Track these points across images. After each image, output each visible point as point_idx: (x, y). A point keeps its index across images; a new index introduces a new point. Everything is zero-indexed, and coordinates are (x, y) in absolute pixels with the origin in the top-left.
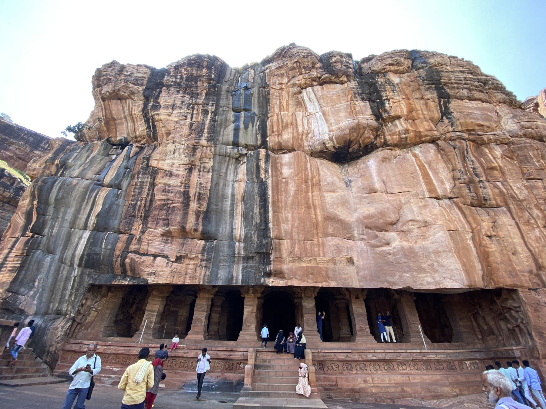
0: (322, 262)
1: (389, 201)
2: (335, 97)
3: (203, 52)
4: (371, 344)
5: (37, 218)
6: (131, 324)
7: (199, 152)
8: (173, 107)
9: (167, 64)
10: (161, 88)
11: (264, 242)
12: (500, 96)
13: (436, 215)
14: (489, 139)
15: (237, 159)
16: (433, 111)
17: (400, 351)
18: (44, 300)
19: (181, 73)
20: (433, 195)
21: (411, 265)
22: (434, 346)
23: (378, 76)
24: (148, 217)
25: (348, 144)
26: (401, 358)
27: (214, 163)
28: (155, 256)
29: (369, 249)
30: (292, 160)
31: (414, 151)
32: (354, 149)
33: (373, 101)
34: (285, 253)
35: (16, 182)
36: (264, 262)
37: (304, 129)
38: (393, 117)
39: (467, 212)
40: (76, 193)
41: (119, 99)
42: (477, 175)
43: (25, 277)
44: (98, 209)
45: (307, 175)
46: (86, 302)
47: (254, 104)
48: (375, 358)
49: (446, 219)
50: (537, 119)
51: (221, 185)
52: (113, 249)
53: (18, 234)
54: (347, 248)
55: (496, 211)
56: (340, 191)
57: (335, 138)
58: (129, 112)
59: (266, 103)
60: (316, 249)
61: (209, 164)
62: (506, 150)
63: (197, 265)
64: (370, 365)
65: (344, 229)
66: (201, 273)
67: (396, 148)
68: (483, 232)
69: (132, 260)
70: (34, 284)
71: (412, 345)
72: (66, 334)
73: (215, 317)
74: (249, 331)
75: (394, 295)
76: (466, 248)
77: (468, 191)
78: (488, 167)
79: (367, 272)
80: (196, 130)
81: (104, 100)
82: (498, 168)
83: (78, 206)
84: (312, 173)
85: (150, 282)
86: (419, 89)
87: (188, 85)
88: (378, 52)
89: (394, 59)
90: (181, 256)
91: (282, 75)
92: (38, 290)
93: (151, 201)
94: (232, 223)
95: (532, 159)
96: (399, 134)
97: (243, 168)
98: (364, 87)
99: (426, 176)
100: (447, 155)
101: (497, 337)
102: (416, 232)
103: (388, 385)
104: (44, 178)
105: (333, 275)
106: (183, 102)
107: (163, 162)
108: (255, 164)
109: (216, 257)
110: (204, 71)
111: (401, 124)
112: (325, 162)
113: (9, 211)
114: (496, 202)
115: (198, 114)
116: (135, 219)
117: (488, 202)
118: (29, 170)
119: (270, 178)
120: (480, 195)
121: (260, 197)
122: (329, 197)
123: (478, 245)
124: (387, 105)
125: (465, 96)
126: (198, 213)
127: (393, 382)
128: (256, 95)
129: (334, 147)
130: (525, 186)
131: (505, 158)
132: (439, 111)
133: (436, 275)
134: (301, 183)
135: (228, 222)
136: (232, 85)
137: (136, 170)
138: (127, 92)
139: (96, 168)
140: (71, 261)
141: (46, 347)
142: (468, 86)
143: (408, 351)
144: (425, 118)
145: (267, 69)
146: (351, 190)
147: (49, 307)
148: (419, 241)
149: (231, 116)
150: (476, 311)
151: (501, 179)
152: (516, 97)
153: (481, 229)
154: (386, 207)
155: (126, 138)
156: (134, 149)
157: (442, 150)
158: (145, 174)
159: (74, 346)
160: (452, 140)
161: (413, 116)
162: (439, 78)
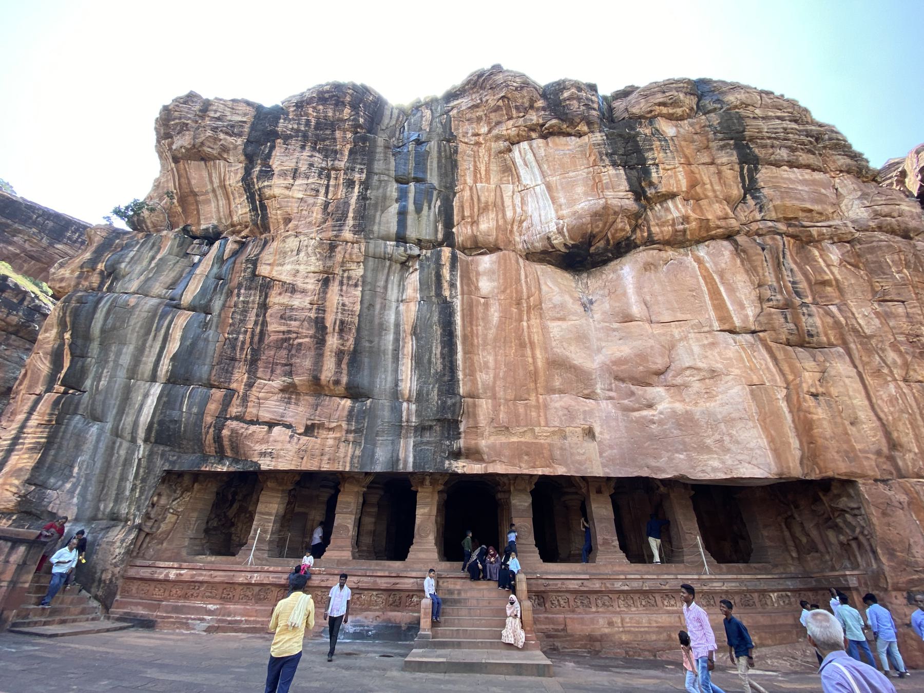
0: (543, 435)
1: (654, 336)
2: (567, 160)
3: (344, 78)
4: (620, 565)
5: (71, 362)
6: (231, 534)
7: (340, 252)
8: (295, 173)
9: (283, 99)
10: (274, 141)
11: (449, 402)
12: (843, 161)
13: (730, 359)
14: (821, 234)
16: (730, 186)
17: (666, 577)
18: (89, 497)
19: (307, 114)
20: (726, 327)
21: (687, 440)
22: (721, 569)
23: (641, 123)
24: (257, 360)
25: (589, 239)
26: (667, 587)
28: (271, 425)
29: (620, 413)
30: (495, 267)
31: (696, 253)
33: (631, 168)
34: (483, 421)
35: (28, 299)
36: (449, 434)
37: (515, 213)
38: (663, 195)
39: (780, 356)
40: (136, 321)
41: (202, 159)
42: (798, 294)
44: (174, 346)
45: (519, 292)
46: (158, 500)
47: (431, 170)
48: (626, 588)
49: (745, 366)
50: (901, 200)
51: (378, 307)
52: (201, 414)
53: (39, 389)
54: (585, 412)
55: (827, 354)
56: (574, 318)
57: (568, 230)
58: (220, 182)
59: (453, 169)
60: (534, 414)
61: (358, 272)
62: (848, 252)
63: (339, 439)
64: (618, 598)
65: (580, 381)
66: (346, 453)
67: (667, 248)
68: (805, 387)
69: (232, 431)
70: (71, 472)
71: (686, 567)
72: (128, 552)
73: (369, 521)
74: (425, 545)
75: (659, 487)
76: (776, 414)
77: (782, 320)
78: (816, 280)
79: (615, 451)
80: (335, 214)
81: (176, 160)
82: (834, 283)
83: (140, 343)
84: (529, 288)
86: (707, 147)
87: (319, 137)
88: (642, 82)
89: (667, 94)
90: (313, 425)
91: (479, 119)
92: (78, 480)
93: (262, 333)
94: (396, 371)
95: (890, 268)
97: (414, 279)
98: (616, 143)
99: (715, 294)
100: (750, 260)
101: (822, 555)
102: (696, 386)
103: (646, 629)
104: (80, 294)
105: (561, 455)
106: (311, 165)
107: (280, 268)
108: (434, 273)
109: (371, 427)
110: (347, 111)
111: (677, 208)
113: (17, 348)
114: (828, 339)
115: (336, 186)
116: (237, 364)
117: (815, 339)
118: (53, 280)
119: (459, 297)
121: (443, 328)
122: (556, 329)
123: (796, 408)
124: (654, 175)
125: (783, 161)
126: (340, 354)
128: (434, 154)
129: (565, 245)
130: (877, 314)
131: (845, 266)
133: (727, 457)
134: (511, 306)
136: (394, 136)
137: (235, 282)
138: (215, 147)
139: (167, 277)
140: (132, 433)
141: (95, 573)
142: (789, 143)
143: (679, 577)
144: (716, 197)
145: (453, 108)
146: (592, 317)
147: (98, 509)
148: (701, 402)
149: (393, 189)
150: (789, 513)
151: (837, 301)
152: (868, 162)
153: (801, 382)
154: (649, 345)
155: (215, 227)
156: (230, 246)
157: (744, 251)
158: (250, 289)
159: (143, 570)
160: (759, 235)
161: (697, 193)
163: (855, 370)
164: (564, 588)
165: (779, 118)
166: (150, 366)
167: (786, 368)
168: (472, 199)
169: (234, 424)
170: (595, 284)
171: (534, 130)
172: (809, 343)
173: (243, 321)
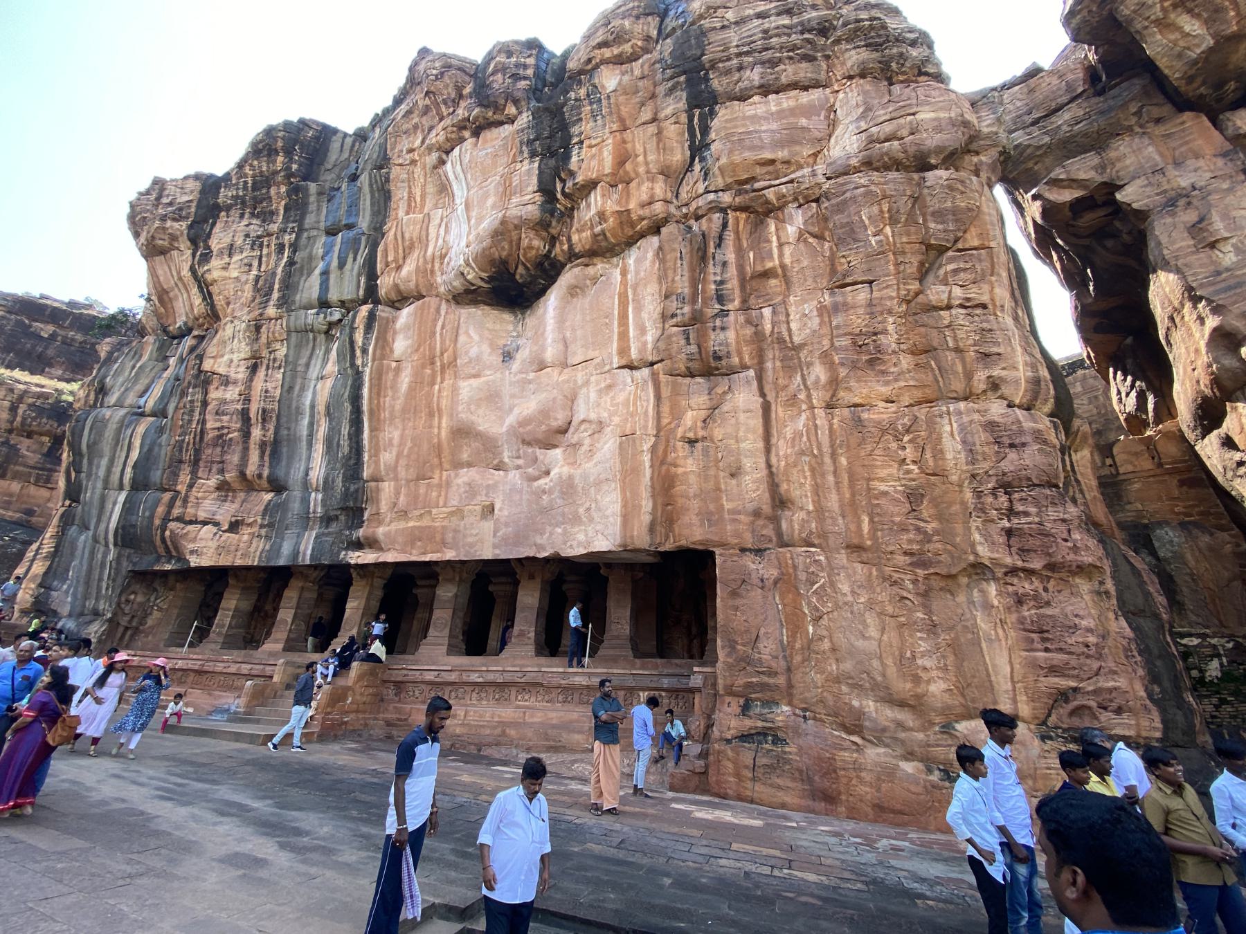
0: (438, 517)
3: (276, 120)
8: (231, 250)
11: (352, 488)
14: (781, 197)
15: (327, 332)
16: (672, 149)
19: (246, 176)
20: (623, 362)
27: (288, 348)
28: (205, 523)
29: (525, 484)
32: (521, 276)
34: (384, 506)
39: (666, 392)
42: (720, 299)
43: (58, 566)
44: (135, 455)
45: (432, 348)
48: (481, 680)
51: (297, 388)
52: (152, 517)
54: (488, 486)
56: (489, 373)
61: (282, 351)
65: (488, 453)
67: (595, 260)
76: (635, 471)
77: (683, 342)
80: (262, 290)
82: (780, 271)
84: (443, 342)
85: (192, 565)
93: (202, 432)
95: (866, 229)
96: (592, 228)
105: (454, 538)
106: (247, 236)
112: (480, 312)
114: (741, 359)
115: (269, 255)
117: (724, 362)
123: (661, 459)
124: (574, 159)
125: (752, 88)
126: (263, 445)
127: (496, 719)
134: (423, 366)
135: (304, 457)
142: (768, 55)
147: (84, 606)
162: (699, 53)
164: (420, 678)
166: (118, 475)
167: (666, 409)
168: (396, 238)
169: (172, 525)
170: (531, 320)
171: (465, 128)
173: (190, 421)
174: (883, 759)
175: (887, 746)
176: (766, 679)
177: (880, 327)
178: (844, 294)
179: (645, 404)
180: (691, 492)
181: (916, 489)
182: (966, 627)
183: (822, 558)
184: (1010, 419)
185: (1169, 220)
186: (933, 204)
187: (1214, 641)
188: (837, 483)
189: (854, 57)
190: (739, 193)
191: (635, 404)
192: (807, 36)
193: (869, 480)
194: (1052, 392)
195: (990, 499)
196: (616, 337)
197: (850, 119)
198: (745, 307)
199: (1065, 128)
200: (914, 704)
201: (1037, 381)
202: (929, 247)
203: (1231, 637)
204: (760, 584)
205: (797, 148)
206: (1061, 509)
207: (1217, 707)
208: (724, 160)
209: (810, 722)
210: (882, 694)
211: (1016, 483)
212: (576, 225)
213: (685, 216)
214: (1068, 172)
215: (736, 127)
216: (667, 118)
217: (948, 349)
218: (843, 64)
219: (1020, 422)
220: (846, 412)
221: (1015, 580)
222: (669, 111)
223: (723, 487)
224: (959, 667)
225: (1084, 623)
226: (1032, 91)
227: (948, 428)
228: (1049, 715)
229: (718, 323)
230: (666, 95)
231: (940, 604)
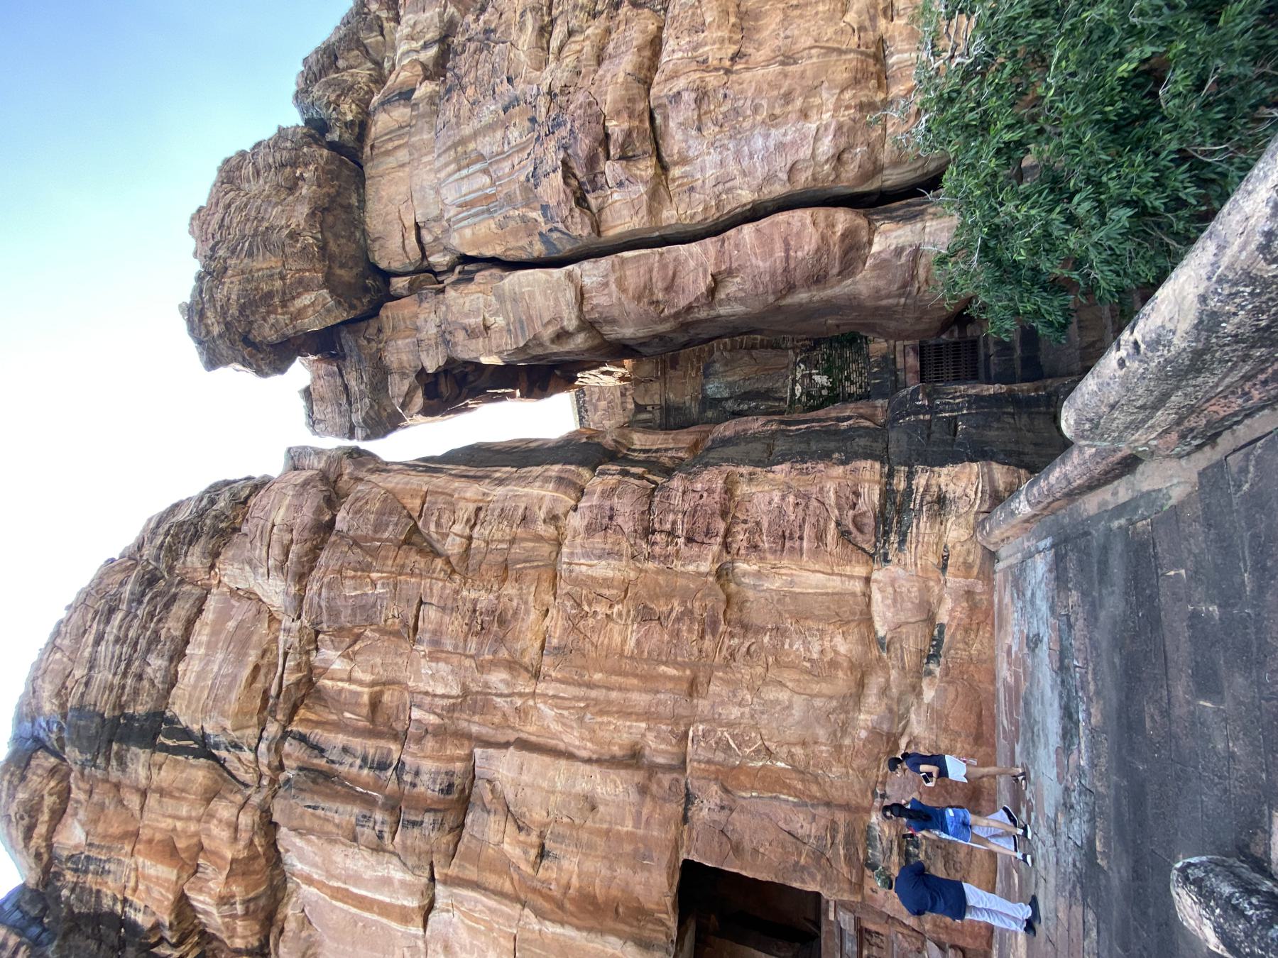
14: (298, 667)
16: (188, 781)
20: (419, 920)
39: (471, 873)
42: (382, 766)
67: (280, 916)
77: (416, 831)
82: (377, 688)
95: (366, 594)
96: (234, 917)
114: (459, 759)
120: (434, 802)
125: (167, 670)
131: (355, 653)
132: (192, 760)
142: (143, 643)
162: (97, 720)
163: (511, 748)
165: (97, 642)
167: (492, 880)
172: (463, 790)
174: (923, 718)
175: (908, 710)
176: (840, 837)
177: (469, 605)
178: (424, 631)
179: (480, 907)
180: (605, 872)
181: (638, 611)
182: (779, 600)
183: (701, 727)
184: (587, 513)
185: (459, 348)
186: (367, 530)
187: (799, 375)
188: (620, 689)
189: (194, 559)
190: (273, 713)
191: (477, 921)
192: (146, 599)
193: (622, 655)
194: (573, 468)
195: (657, 549)
196: (384, 921)
197: (251, 579)
198: (401, 737)
199: (362, 387)
200: (861, 674)
201: (560, 480)
202: (407, 542)
203: (796, 364)
204: (727, 812)
205: (255, 638)
206: (674, 493)
207: (852, 383)
208: (228, 724)
209: (888, 790)
210: (851, 703)
211: (646, 524)
212: (224, 936)
213: (273, 781)
214: (399, 396)
215: (199, 700)
216: (149, 778)
217: (509, 549)
218: (195, 570)
219: (591, 506)
220: (547, 660)
221: (734, 546)
222: (142, 773)
223: (605, 826)
224: (819, 619)
225: (776, 499)
226: (322, 399)
227: (584, 568)
228: (863, 550)
229: (408, 778)
230: (124, 771)
231: (756, 616)
